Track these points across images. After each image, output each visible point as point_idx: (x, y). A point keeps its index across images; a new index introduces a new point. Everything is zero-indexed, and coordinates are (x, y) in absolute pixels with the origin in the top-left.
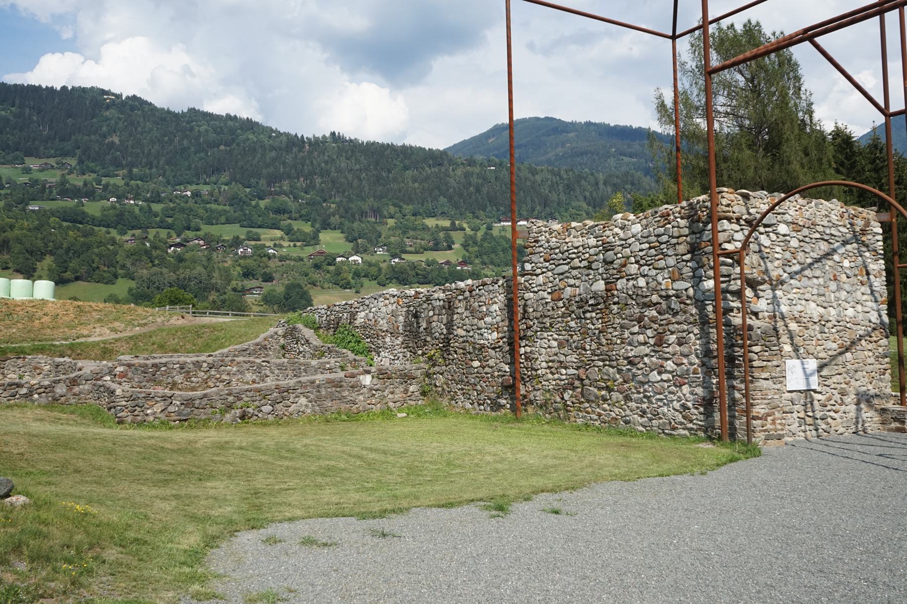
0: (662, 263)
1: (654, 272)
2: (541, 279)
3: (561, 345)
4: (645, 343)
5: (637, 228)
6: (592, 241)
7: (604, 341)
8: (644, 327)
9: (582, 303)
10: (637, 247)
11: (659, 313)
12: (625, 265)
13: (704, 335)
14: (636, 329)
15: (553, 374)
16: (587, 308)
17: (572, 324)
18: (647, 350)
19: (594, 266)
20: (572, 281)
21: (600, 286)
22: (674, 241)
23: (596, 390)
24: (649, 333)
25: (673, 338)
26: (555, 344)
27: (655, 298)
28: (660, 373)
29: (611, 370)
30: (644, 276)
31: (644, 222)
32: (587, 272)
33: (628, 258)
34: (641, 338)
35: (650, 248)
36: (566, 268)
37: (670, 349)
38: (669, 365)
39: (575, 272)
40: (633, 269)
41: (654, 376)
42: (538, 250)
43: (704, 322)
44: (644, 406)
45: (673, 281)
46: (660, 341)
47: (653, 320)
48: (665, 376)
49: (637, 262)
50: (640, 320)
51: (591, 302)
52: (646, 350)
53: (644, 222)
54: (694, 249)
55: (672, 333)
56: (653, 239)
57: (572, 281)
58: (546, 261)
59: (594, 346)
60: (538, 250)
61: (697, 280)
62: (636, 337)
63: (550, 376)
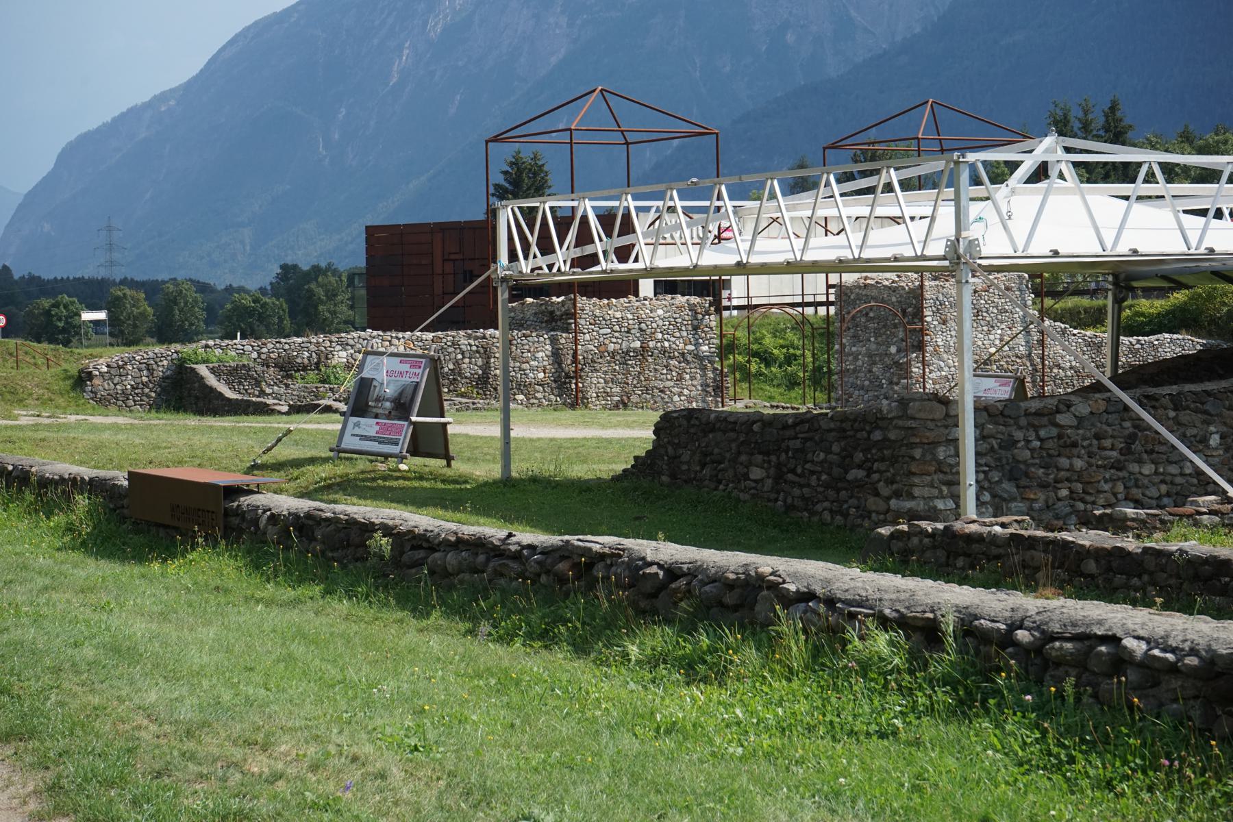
0: (678, 334)
1: (673, 339)
2: (587, 337)
3: (606, 382)
4: (671, 380)
5: (660, 312)
6: (630, 316)
8: (671, 370)
10: (661, 323)
11: (679, 362)
13: (704, 375)
14: (665, 371)
16: (628, 357)
17: (617, 368)
18: (672, 384)
19: (632, 331)
20: (614, 340)
21: (638, 344)
25: (687, 377)
28: (679, 396)
36: (609, 331)
38: (686, 392)
39: (617, 334)
40: (660, 336)
41: (676, 398)
42: (583, 316)
43: (704, 368)
45: (686, 345)
46: (680, 378)
48: (683, 398)
51: (632, 354)
52: (672, 384)
54: (696, 328)
57: (614, 340)
58: (591, 324)
60: (583, 316)
61: (697, 344)
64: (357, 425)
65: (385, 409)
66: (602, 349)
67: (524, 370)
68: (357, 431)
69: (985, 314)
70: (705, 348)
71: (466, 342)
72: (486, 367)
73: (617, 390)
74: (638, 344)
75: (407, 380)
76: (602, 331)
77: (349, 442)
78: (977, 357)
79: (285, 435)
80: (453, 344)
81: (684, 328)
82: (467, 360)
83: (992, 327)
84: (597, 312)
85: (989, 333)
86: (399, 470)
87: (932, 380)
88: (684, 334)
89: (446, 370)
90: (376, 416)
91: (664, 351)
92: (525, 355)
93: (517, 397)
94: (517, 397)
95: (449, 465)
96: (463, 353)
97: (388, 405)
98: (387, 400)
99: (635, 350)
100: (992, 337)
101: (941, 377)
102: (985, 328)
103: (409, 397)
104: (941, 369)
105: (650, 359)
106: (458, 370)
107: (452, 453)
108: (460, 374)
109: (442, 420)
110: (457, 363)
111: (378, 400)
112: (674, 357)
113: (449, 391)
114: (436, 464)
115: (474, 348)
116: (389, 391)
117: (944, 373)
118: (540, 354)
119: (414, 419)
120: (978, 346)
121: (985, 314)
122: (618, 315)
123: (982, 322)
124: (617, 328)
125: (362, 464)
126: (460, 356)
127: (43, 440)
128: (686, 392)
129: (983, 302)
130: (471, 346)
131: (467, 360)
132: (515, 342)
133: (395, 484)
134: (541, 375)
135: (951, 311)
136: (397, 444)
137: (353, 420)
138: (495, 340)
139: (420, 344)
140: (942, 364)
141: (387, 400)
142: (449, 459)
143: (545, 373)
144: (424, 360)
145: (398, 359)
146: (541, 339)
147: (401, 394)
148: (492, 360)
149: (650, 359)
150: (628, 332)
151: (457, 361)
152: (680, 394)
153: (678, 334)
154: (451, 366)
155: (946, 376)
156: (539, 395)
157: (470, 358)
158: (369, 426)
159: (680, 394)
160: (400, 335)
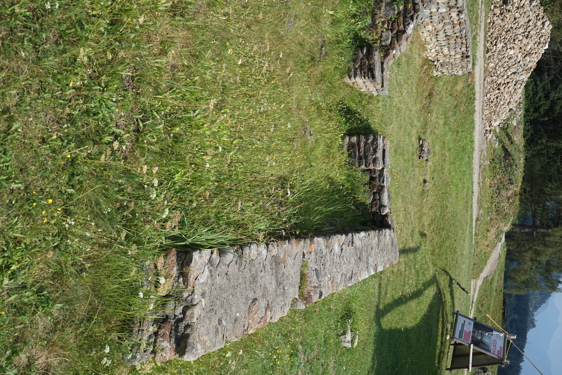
64: (470, 324)
65: (477, 336)
68: (466, 323)
75: (492, 348)
77: (461, 320)
79: (466, 292)
86: (447, 334)
90: (473, 332)
95: (447, 369)
97: (479, 338)
98: (482, 338)
103: (482, 346)
107: (453, 371)
109: (470, 365)
111: (482, 334)
114: (447, 361)
116: (486, 340)
119: (472, 345)
125: (450, 318)
127: (467, 211)
133: (440, 327)
136: (459, 337)
137: (472, 323)
141: (482, 338)
142: (450, 369)
144: (502, 356)
145: (502, 346)
147: (484, 344)
158: (469, 328)
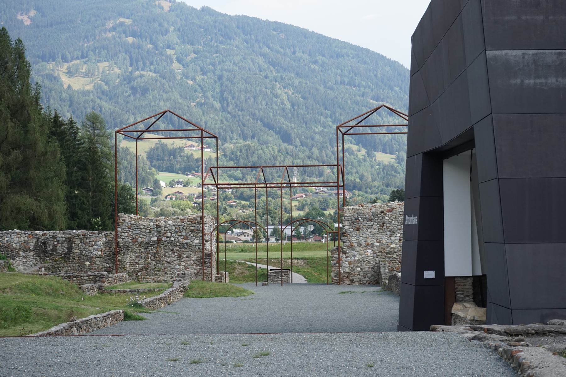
0: (180, 234)
2: (126, 234)
3: (137, 257)
5: (170, 222)
6: (151, 224)
7: (157, 256)
9: (147, 243)
11: (180, 248)
12: (166, 233)
14: (171, 253)
15: (132, 266)
17: (143, 250)
19: (152, 232)
20: (142, 236)
21: (155, 239)
22: (185, 228)
23: (153, 271)
24: (176, 254)
25: (185, 256)
26: (134, 257)
27: (178, 244)
29: (160, 265)
30: (173, 237)
31: (173, 221)
32: (149, 234)
33: (167, 231)
34: (173, 255)
35: (176, 229)
36: (139, 232)
37: (184, 259)
39: (143, 233)
40: (169, 234)
41: (178, 267)
42: (125, 224)
44: (172, 276)
45: (185, 239)
46: (180, 256)
47: (177, 250)
49: (170, 233)
50: (172, 250)
51: (151, 244)
53: (173, 221)
55: (184, 254)
56: (177, 226)
57: (142, 236)
58: (128, 228)
59: (152, 258)
60: (125, 224)
62: (170, 255)
63: (131, 267)
66: (134, 240)
67: (90, 250)
69: (388, 225)
70: (196, 241)
71: (60, 236)
72: (70, 248)
73: (143, 261)
74: (155, 239)
76: (134, 232)
78: (382, 250)
80: (53, 237)
81: (184, 231)
82: (60, 245)
83: (394, 232)
84: (133, 222)
85: (390, 236)
87: (348, 262)
88: (184, 234)
89: (48, 249)
91: (171, 242)
92: (91, 243)
93: (86, 263)
94: (86, 263)
96: (58, 241)
99: (153, 241)
100: (392, 238)
101: (355, 261)
102: (388, 233)
104: (355, 256)
105: (162, 246)
106: (54, 249)
108: (56, 252)
110: (54, 246)
112: (176, 246)
113: (50, 259)
115: (64, 239)
117: (356, 258)
118: (100, 242)
120: (383, 243)
121: (388, 225)
122: (144, 224)
123: (386, 230)
124: (144, 230)
126: (56, 243)
128: (183, 264)
129: (387, 218)
130: (62, 238)
131: (60, 245)
132: (86, 236)
134: (100, 253)
135: (363, 223)
138: (75, 235)
139: (36, 236)
140: (355, 253)
143: (102, 252)
146: (101, 235)
148: (73, 245)
149: (162, 246)
150: (150, 232)
151: (55, 245)
152: (180, 265)
153: (180, 234)
154: (51, 247)
155: (358, 260)
156: (97, 263)
157: (62, 244)
159: (180, 265)
160: (26, 232)
